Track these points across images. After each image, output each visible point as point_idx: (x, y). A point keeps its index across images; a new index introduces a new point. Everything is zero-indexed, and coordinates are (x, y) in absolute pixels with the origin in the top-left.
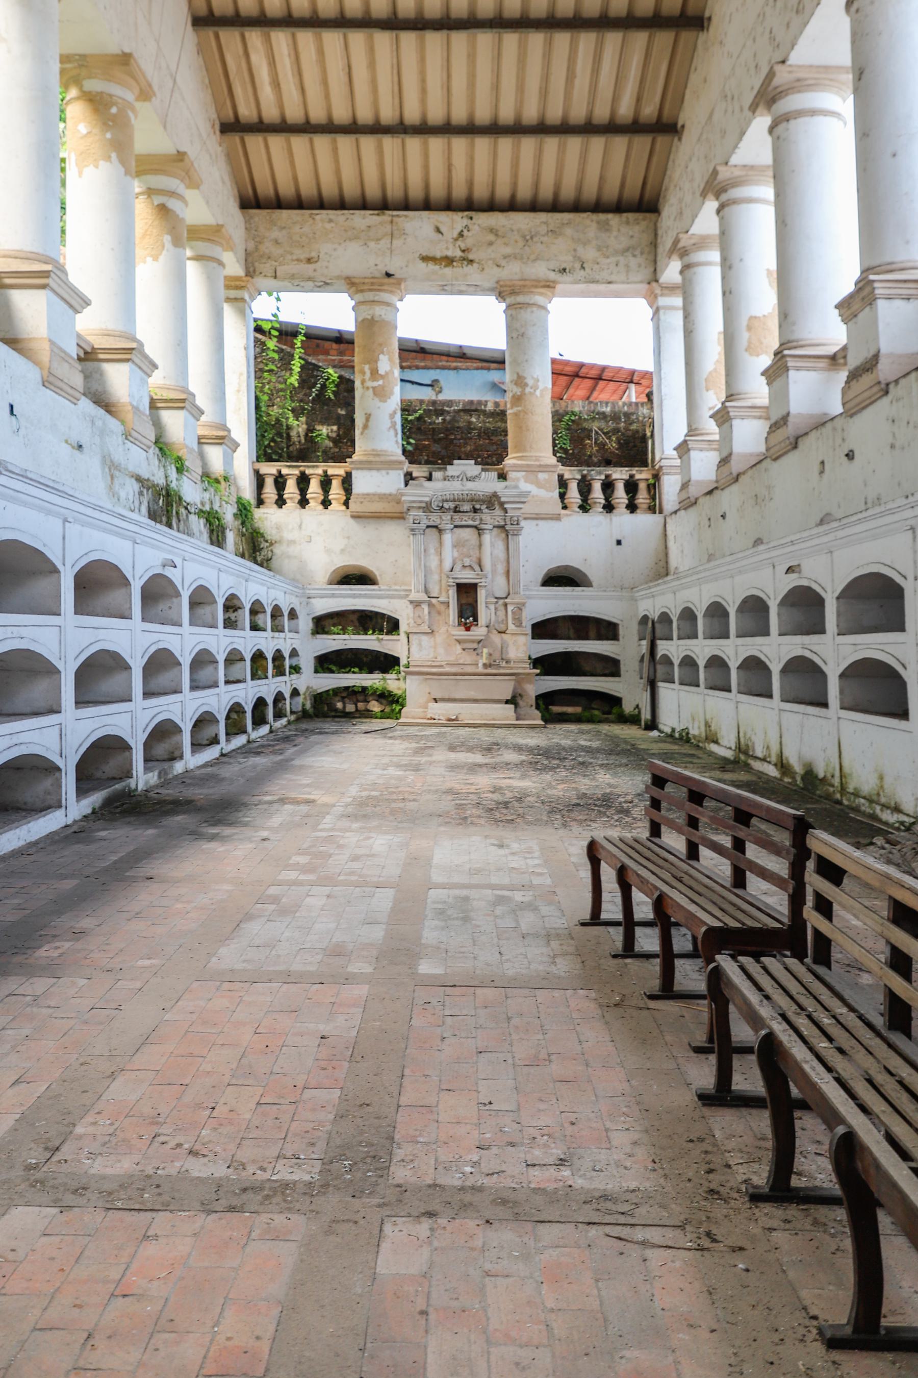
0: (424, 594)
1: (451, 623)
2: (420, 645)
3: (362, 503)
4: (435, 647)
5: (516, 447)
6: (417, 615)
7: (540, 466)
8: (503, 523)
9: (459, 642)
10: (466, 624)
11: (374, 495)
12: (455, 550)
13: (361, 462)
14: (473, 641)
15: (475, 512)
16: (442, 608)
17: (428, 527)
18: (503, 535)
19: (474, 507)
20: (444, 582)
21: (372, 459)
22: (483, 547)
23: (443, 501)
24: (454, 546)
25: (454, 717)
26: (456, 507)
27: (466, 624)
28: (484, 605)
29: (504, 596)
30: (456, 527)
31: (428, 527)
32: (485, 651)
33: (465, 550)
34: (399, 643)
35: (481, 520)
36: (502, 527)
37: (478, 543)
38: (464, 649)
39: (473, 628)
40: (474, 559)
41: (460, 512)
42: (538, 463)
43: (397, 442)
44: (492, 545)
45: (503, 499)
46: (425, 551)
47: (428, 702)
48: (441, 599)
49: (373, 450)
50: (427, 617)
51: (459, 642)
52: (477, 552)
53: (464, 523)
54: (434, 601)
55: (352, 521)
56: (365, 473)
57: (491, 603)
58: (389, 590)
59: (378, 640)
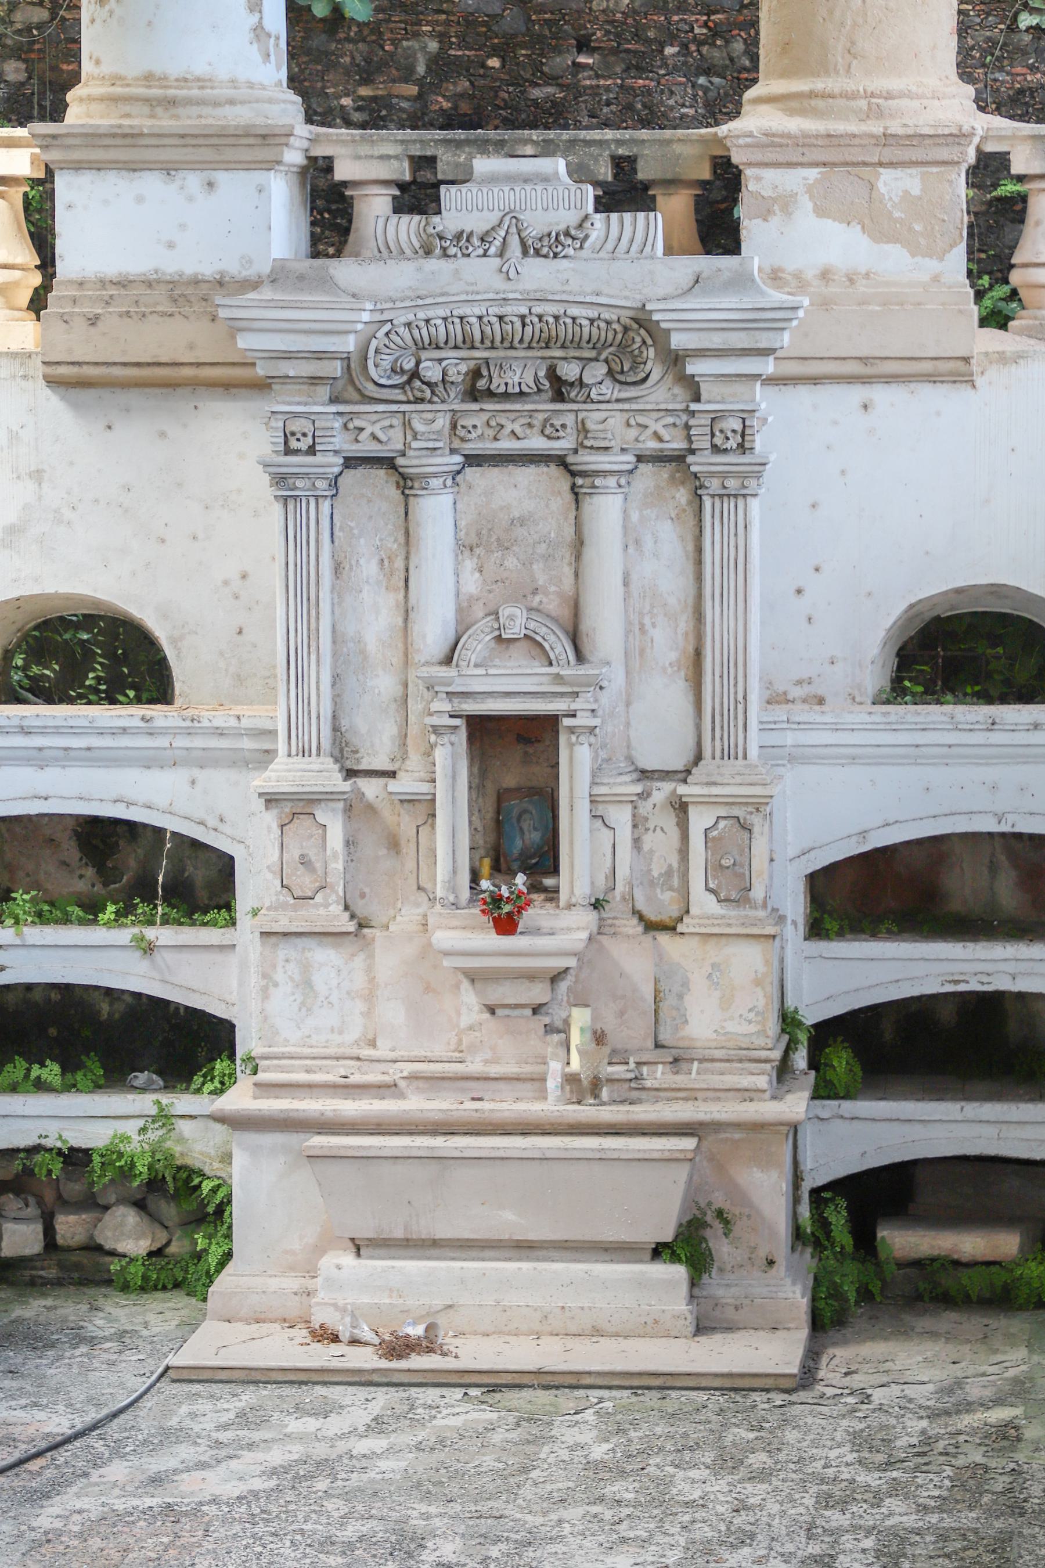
0: (329, 764)
1: (440, 893)
2: (306, 984)
3: (93, 321)
4: (370, 997)
5: (786, 47)
6: (294, 852)
7: (887, 139)
8: (678, 444)
9: (473, 977)
10: (497, 900)
11: (149, 284)
12: (469, 564)
13: (92, 138)
14: (530, 976)
15: (559, 397)
16: (406, 824)
17: (351, 462)
18: (682, 495)
19: (553, 375)
20: (415, 707)
21: (140, 121)
22: (589, 553)
23: (420, 346)
24: (465, 547)
25: (417, 1331)
26: (476, 374)
27: (497, 900)
28: (583, 807)
29: (678, 764)
30: (474, 460)
31: (351, 462)
32: (580, 1018)
33: (511, 562)
34: (233, 960)
35: (583, 430)
36: (678, 459)
37: (569, 531)
38: (492, 1010)
39: (531, 916)
40: (552, 604)
41: (490, 394)
42: (875, 128)
43: (259, 32)
44: (631, 541)
45: (677, 341)
46: (338, 569)
47: (320, 1249)
48: (406, 784)
49: (149, 78)
50: (339, 865)
51: (473, 977)
52: (568, 572)
53: (507, 445)
54: (371, 788)
55: (51, 401)
56: (113, 183)
57: (618, 800)
58: (189, 733)
59: (148, 949)
